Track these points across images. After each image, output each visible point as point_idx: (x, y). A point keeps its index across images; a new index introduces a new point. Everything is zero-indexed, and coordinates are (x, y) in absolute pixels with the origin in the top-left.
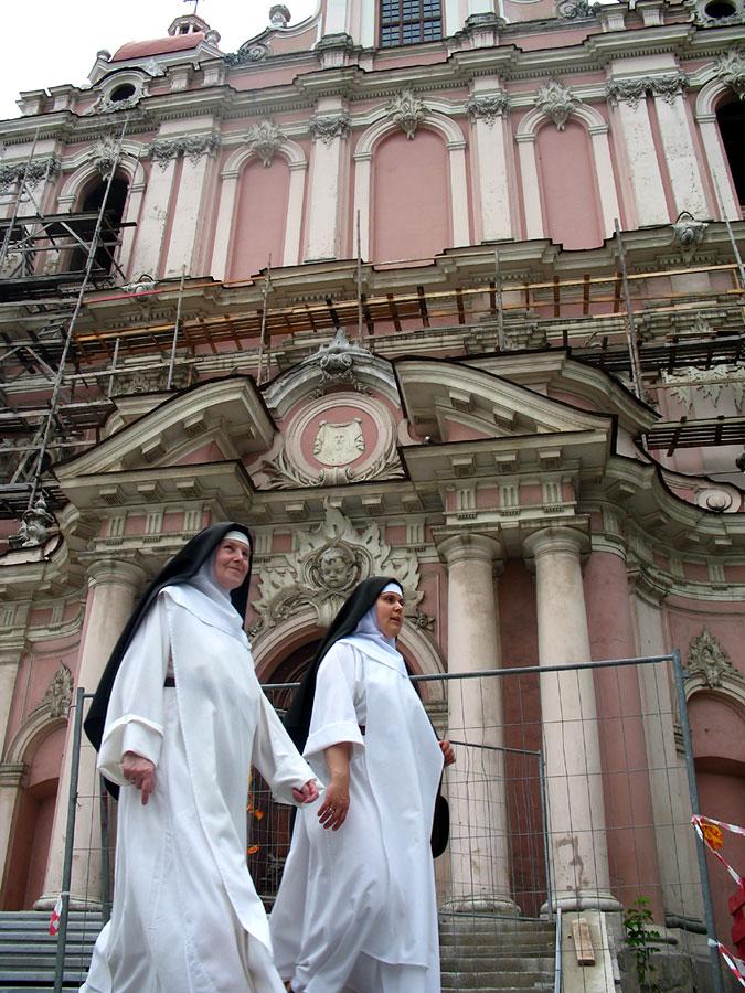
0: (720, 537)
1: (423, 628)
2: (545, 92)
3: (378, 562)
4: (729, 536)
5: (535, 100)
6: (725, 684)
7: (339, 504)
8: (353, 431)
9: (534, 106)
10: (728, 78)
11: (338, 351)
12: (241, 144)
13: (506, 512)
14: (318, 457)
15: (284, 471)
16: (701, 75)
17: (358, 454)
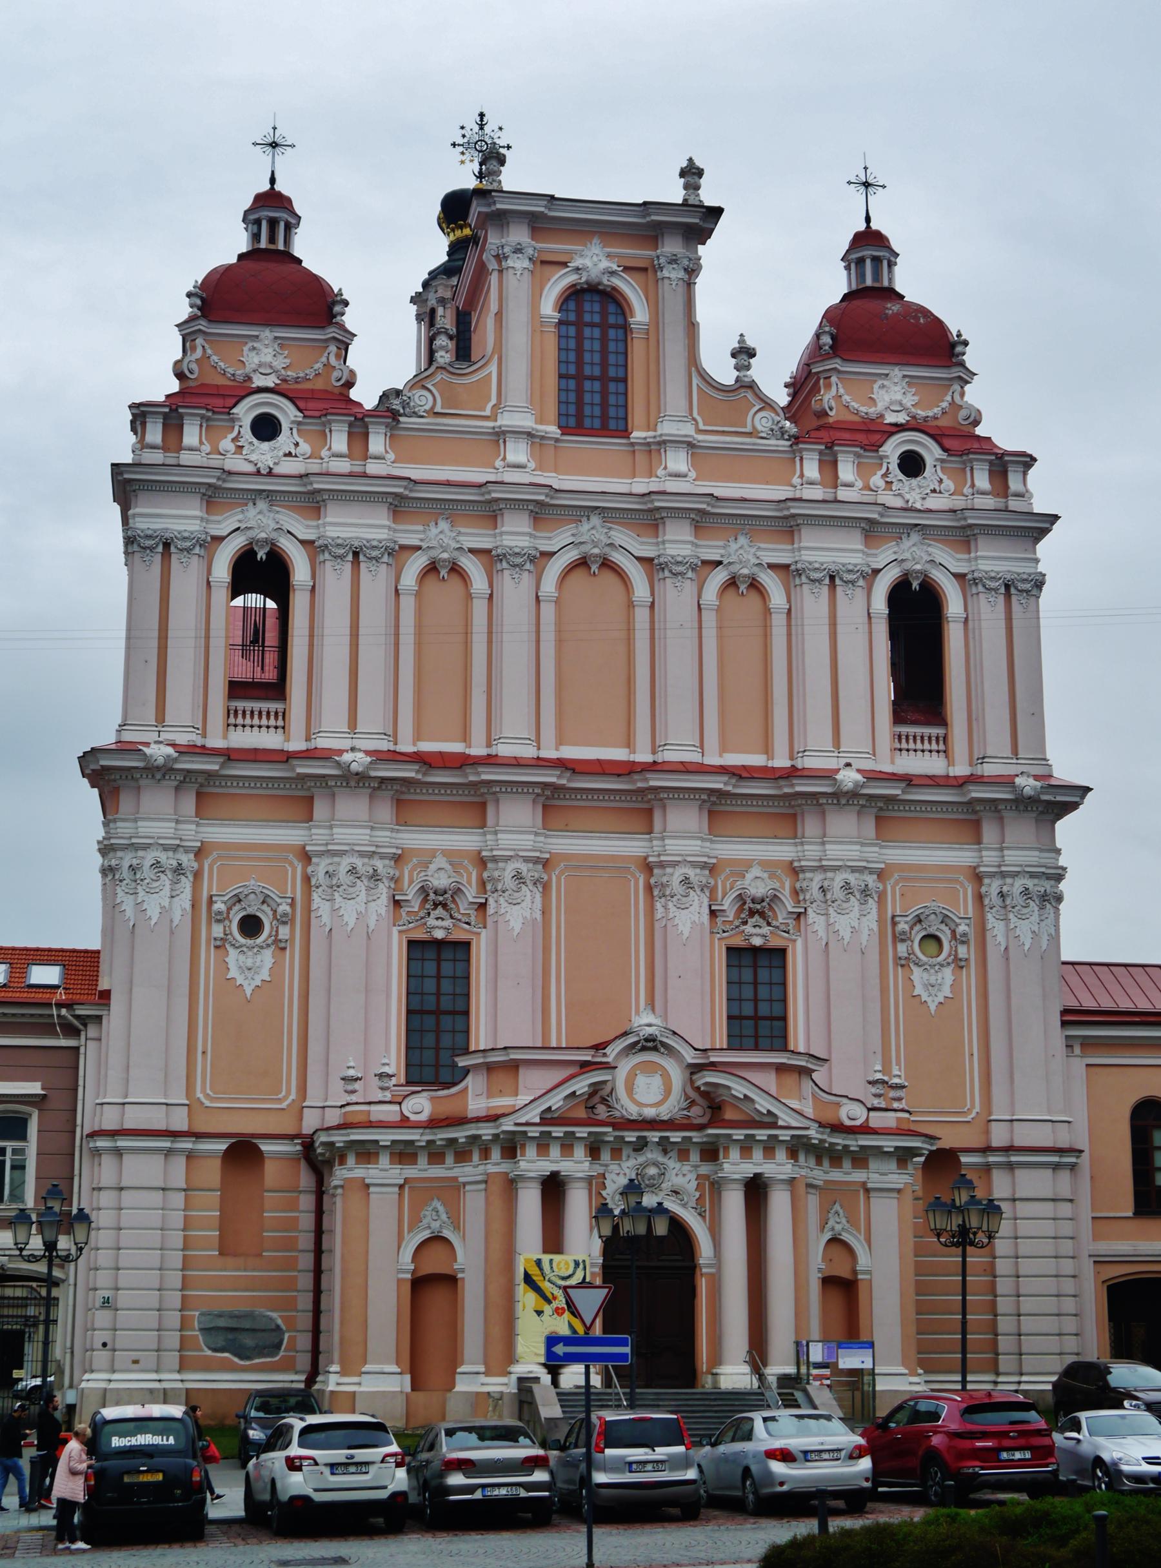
0: (853, 1146)
1: (700, 1214)
2: (734, 546)
3: (674, 1172)
4: (858, 1146)
5: (722, 556)
6: (843, 1234)
7: (657, 1140)
8: (656, 1081)
9: (720, 563)
10: (907, 566)
11: (650, 1025)
12: (419, 548)
13: (757, 1164)
14: (635, 1096)
15: (616, 1106)
16: (883, 555)
17: (661, 1097)
